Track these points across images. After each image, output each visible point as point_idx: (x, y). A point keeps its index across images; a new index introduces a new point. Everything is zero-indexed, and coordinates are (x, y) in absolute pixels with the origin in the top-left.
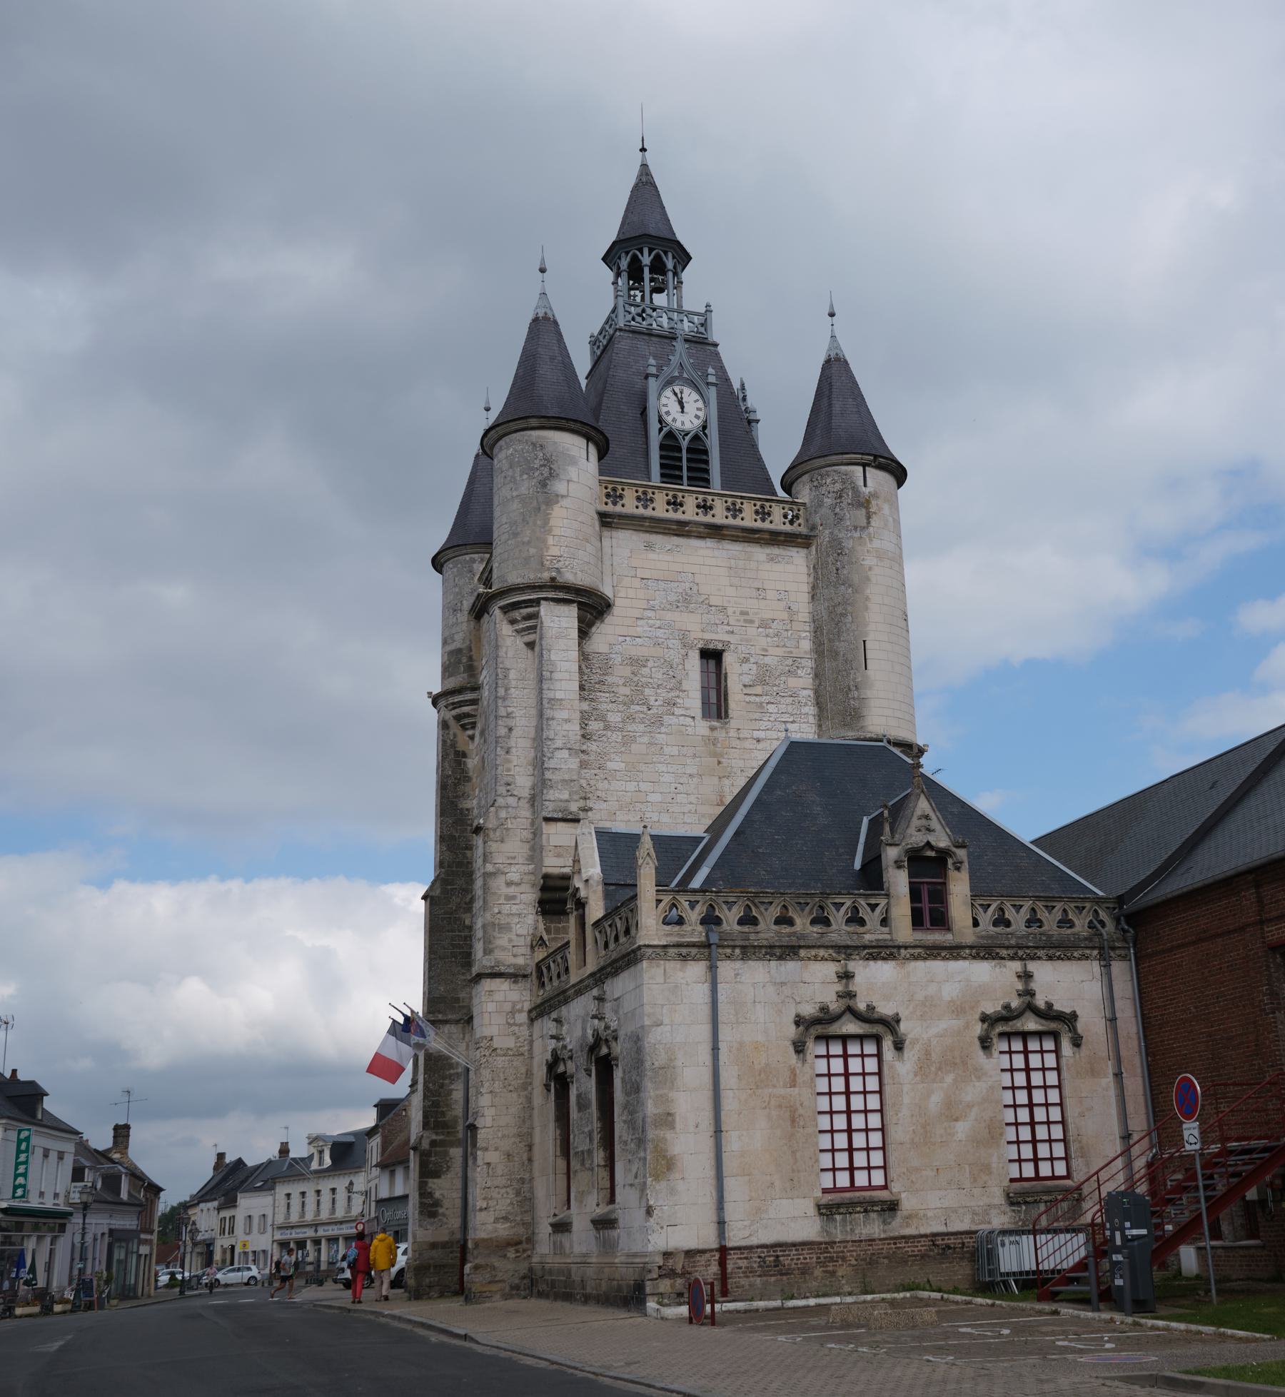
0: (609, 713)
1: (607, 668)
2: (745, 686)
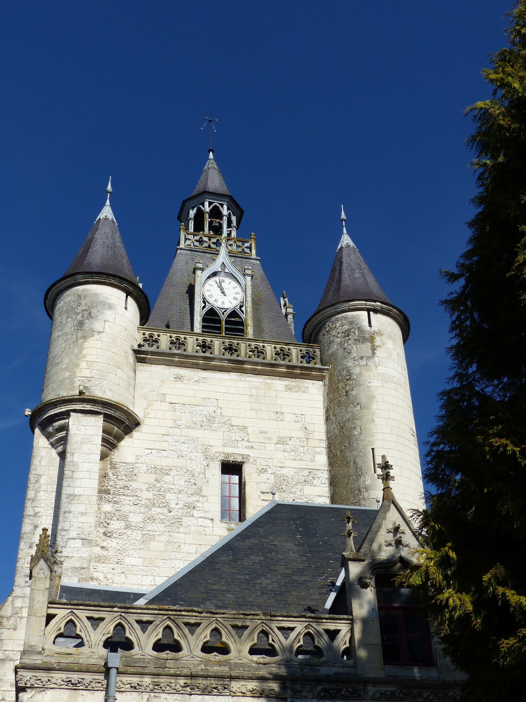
0: (131, 514)
1: (132, 475)
2: (263, 493)
